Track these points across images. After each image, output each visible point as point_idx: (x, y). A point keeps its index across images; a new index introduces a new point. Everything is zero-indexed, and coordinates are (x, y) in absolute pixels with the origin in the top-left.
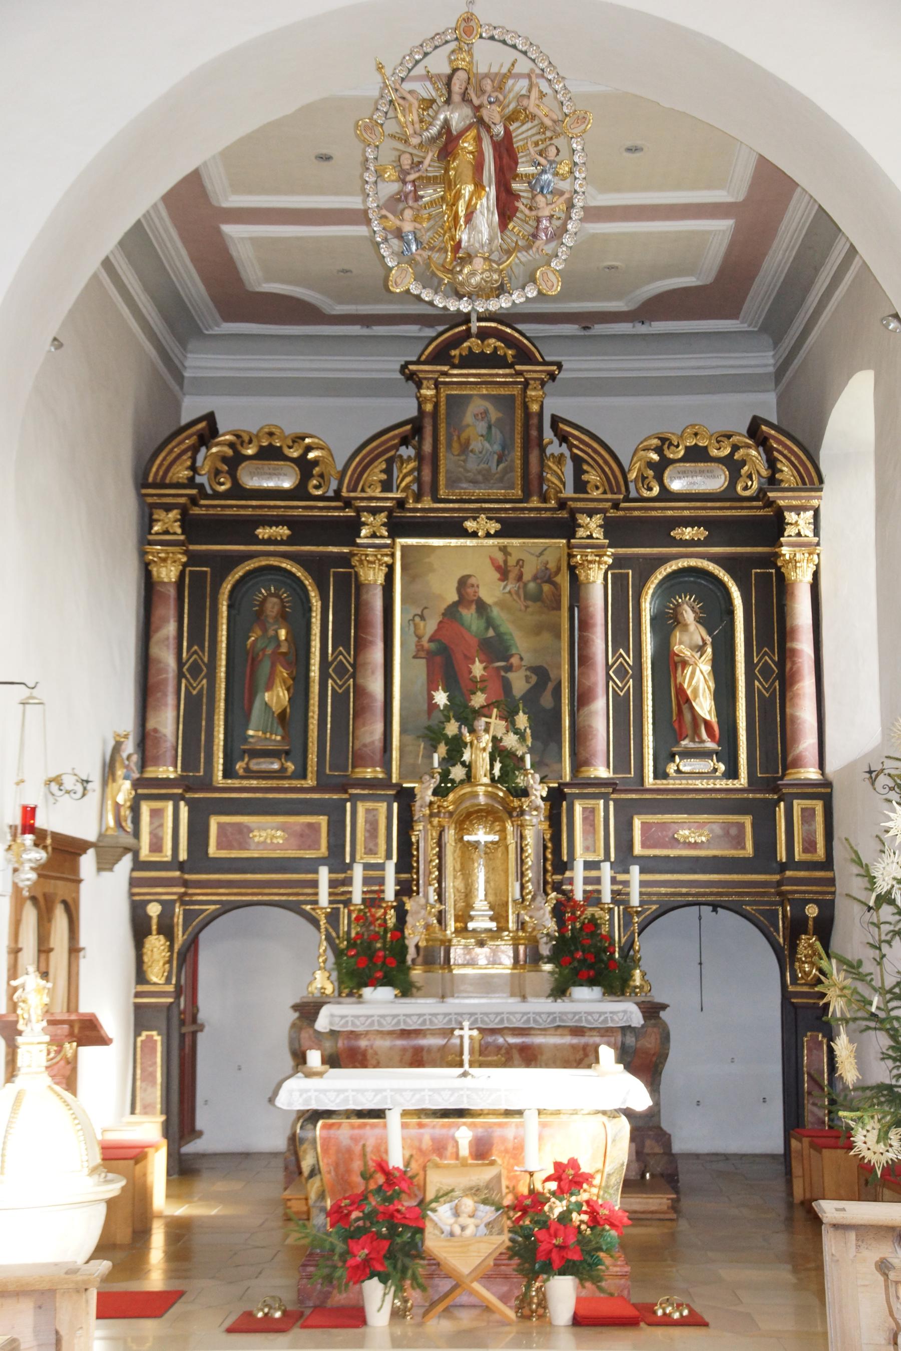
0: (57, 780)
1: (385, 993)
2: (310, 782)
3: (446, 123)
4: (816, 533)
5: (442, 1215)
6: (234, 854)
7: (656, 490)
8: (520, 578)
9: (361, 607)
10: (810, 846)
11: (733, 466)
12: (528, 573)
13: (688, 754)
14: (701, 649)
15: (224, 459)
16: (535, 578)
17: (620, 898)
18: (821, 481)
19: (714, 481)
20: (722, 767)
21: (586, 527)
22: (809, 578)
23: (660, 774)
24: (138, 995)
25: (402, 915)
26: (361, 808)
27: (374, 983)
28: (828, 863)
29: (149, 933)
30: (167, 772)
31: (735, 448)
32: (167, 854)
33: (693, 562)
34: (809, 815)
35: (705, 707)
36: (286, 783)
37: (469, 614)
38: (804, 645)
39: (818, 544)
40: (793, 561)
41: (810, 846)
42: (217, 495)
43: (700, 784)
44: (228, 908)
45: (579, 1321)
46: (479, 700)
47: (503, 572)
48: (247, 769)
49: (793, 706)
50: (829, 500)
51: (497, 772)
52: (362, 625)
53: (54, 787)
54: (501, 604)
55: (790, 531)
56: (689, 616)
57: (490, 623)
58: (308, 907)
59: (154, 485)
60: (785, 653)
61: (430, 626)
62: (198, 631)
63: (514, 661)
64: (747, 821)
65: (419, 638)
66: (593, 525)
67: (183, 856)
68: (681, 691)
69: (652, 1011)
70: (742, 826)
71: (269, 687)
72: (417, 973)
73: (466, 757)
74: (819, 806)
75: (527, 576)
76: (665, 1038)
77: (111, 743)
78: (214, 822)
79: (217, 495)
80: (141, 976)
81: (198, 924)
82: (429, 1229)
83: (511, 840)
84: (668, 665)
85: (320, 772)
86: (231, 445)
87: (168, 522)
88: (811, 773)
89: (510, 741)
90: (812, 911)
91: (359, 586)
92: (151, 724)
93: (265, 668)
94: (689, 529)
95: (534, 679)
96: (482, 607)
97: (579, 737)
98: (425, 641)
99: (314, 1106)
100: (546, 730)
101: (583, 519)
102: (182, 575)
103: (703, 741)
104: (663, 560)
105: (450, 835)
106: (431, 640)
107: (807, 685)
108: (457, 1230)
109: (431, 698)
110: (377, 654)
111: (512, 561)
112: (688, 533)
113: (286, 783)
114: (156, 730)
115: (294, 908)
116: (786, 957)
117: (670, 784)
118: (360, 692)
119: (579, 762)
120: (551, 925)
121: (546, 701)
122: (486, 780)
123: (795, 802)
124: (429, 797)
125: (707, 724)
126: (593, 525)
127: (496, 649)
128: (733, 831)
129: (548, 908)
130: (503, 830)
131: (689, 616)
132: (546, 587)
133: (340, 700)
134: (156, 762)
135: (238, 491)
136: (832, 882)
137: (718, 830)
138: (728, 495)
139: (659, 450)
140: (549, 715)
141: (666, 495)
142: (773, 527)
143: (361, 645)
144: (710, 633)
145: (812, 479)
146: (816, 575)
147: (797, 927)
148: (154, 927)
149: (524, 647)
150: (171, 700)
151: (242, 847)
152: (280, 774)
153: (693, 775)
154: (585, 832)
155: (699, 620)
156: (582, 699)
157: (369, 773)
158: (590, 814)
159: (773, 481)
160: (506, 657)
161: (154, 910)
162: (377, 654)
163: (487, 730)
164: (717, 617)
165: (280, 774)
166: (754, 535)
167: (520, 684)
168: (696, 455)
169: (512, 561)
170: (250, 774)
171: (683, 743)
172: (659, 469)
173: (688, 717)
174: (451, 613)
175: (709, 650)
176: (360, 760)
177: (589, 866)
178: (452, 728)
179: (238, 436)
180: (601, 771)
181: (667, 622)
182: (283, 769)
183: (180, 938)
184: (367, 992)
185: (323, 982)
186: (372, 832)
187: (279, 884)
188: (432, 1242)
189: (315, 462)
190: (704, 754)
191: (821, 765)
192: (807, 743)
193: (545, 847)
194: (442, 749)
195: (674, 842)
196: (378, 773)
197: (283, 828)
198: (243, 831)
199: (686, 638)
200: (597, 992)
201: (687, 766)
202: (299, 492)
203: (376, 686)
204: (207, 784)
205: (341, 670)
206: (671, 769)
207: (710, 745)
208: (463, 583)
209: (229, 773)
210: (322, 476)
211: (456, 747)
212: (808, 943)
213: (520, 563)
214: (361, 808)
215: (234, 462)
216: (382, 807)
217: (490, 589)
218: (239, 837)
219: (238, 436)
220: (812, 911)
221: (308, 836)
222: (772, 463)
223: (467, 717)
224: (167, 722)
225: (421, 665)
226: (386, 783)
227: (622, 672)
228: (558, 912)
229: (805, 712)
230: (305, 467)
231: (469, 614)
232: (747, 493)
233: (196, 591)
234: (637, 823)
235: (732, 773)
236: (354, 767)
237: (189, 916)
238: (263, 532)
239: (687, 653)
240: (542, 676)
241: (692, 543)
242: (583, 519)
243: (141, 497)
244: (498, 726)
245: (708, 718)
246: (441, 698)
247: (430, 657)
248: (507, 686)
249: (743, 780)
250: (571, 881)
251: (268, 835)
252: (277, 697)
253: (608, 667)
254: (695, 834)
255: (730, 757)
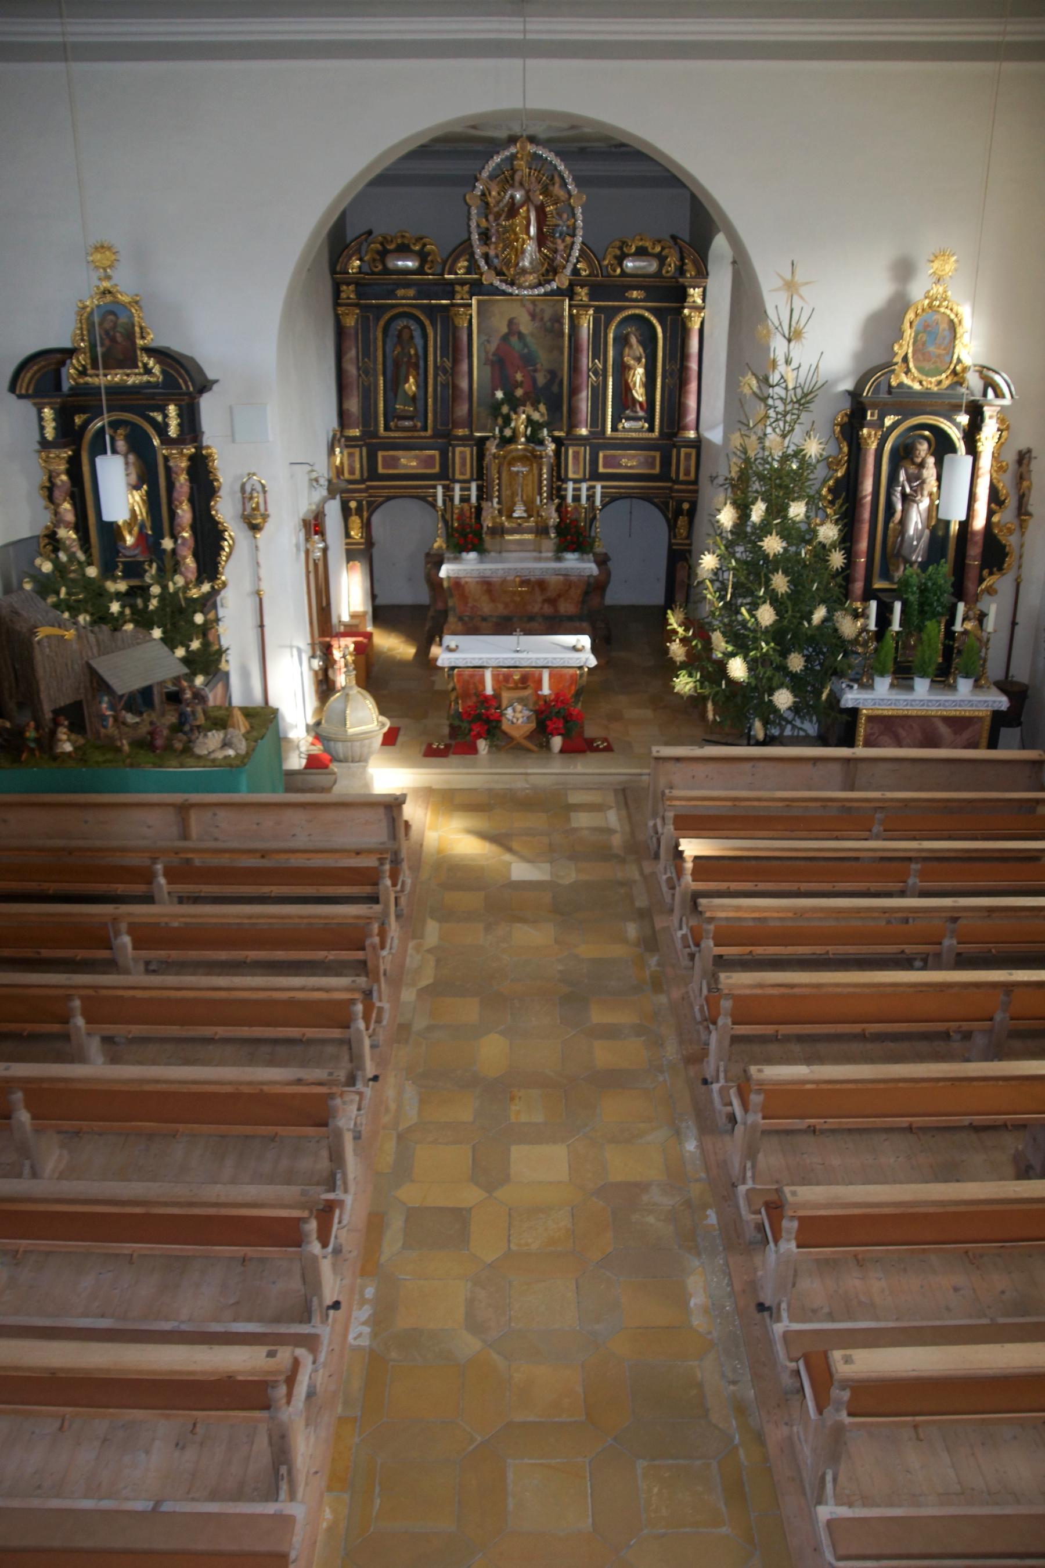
0: (316, 480)
1: (472, 555)
2: (429, 433)
3: (512, 197)
4: (704, 300)
5: (509, 712)
6: (391, 471)
7: (619, 271)
8: (542, 319)
9: (456, 339)
10: (687, 473)
11: (662, 259)
12: (547, 316)
13: (628, 419)
14: (639, 360)
15: (378, 252)
16: (550, 319)
17: (591, 498)
18: (707, 274)
19: (652, 266)
20: (646, 425)
21: (579, 294)
22: (697, 326)
23: (614, 429)
24: (347, 544)
25: (479, 510)
26: (458, 449)
27: (468, 551)
28: (696, 482)
29: (351, 515)
30: (356, 432)
31: (663, 248)
32: (357, 476)
33: (637, 311)
34: (688, 456)
35: (639, 394)
36: (416, 434)
37: (514, 340)
38: (694, 365)
39: (704, 308)
40: (690, 316)
41: (687, 473)
42: (373, 273)
43: (634, 435)
44: (389, 498)
45: (562, 751)
46: (519, 392)
47: (533, 316)
48: (396, 426)
49: (686, 398)
50: (711, 282)
51: (529, 432)
52: (456, 350)
53: (315, 484)
54: (532, 335)
55: (690, 299)
56: (633, 340)
57: (526, 345)
58: (430, 499)
59: (340, 273)
60: (684, 369)
61: (493, 347)
62: (367, 351)
63: (538, 366)
64: (658, 454)
65: (487, 353)
66: (583, 294)
67: (365, 475)
68: (627, 384)
69: (602, 561)
70: (654, 458)
71: (407, 381)
72: (487, 538)
73: (513, 425)
74: (693, 452)
75: (546, 318)
76: (609, 574)
77: (331, 434)
78: (380, 454)
79: (373, 273)
80: (348, 535)
81: (373, 507)
82: (504, 721)
83: (536, 471)
84: (622, 370)
85: (435, 427)
86: (382, 244)
87: (349, 292)
88: (692, 434)
89: (536, 416)
90: (686, 506)
91: (456, 329)
92: (345, 406)
93: (403, 369)
94: (635, 292)
95: (549, 377)
96: (521, 336)
97: (573, 411)
98: (491, 357)
99: (453, 665)
100: (555, 407)
101: (578, 289)
102: (357, 320)
103: (636, 412)
104: (621, 309)
105: (505, 469)
106: (494, 354)
107: (693, 386)
108: (515, 720)
109: (494, 395)
110: (465, 367)
111: (538, 310)
112: (635, 294)
113: (416, 434)
114: (348, 410)
115: (423, 499)
116: (672, 526)
117: (620, 435)
118: (455, 387)
119: (573, 425)
120: (555, 515)
121: (555, 389)
122: (523, 440)
123: (683, 450)
124: (494, 450)
125: (641, 404)
126: (583, 294)
127: (528, 360)
128: (650, 460)
129: (553, 508)
130: (531, 465)
131: (633, 340)
132: (556, 325)
133: (444, 386)
134: (350, 427)
135: (386, 271)
136: (696, 491)
137: (642, 459)
138: (658, 274)
139: (621, 248)
140: (557, 399)
141: (624, 274)
142: (681, 295)
143: (456, 362)
144: (645, 351)
145: (703, 273)
146: (702, 324)
147: (679, 512)
148: (354, 511)
149: (544, 359)
150: (355, 392)
151: (395, 467)
152: (413, 429)
153: (630, 430)
154: (574, 464)
155: (640, 342)
156: (574, 391)
157: (460, 432)
158: (576, 455)
159: (681, 271)
160: (535, 365)
161: (353, 505)
162: (465, 367)
163: (524, 412)
164: (649, 341)
165: (413, 429)
166: (671, 297)
167: (541, 379)
168: (641, 253)
169: (538, 310)
170: (398, 429)
171: (627, 412)
172: (620, 259)
173: (629, 397)
174: (505, 338)
175: (644, 360)
176: (456, 425)
177: (575, 481)
178: (505, 409)
179: (385, 238)
180: (584, 431)
181: (622, 341)
182: (415, 426)
183: (365, 514)
184: (464, 555)
185: (439, 543)
186: (463, 464)
187: (414, 488)
188: (505, 726)
189: (429, 254)
190: (637, 419)
191: (697, 429)
192: (691, 417)
193: (553, 470)
194: (500, 421)
195: (620, 466)
196: (466, 432)
197: (416, 457)
198: (396, 459)
199: (631, 353)
200: (576, 555)
201: (627, 425)
202: (420, 271)
203: (464, 384)
204: (375, 435)
205: (445, 371)
206: (620, 426)
207: (641, 414)
208: (511, 323)
209: (387, 428)
210: (432, 261)
211: (507, 420)
212: (682, 521)
213: (542, 311)
214: (458, 449)
215: (383, 254)
216: (467, 450)
217: (526, 325)
218: (394, 462)
219: (385, 238)
220: (686, 506)
221: (429, 462)
222: (682, 259)
223: (515, 404)
224: (353, 405)
225: (488, 369)
226: (470, 437)
227: (596, 373)
228: (559, 509)
229: (692, 403)
230: (423, 257)
231: (514, 340)
232: (669, 275)
233: (365, 324)
234: (601, 455)
235: (651, 429)
236: (453, 428)
237: (369, 504)
238: (400, 292)
239: (632, 362)
240: (553, 375)
241: (636, 300)
242: (578, 289)
243: (333, 279)
244: (529, 409)
245: (641, 399)
246: (499, 395)
247: (493, 364)
248: (534, 381)
249: (656, 433)
250: (566, 489)
251: (409, 462)
252: (411, 386)
253: (589, 370)
254: (630, 462)
255: (651, 420)
